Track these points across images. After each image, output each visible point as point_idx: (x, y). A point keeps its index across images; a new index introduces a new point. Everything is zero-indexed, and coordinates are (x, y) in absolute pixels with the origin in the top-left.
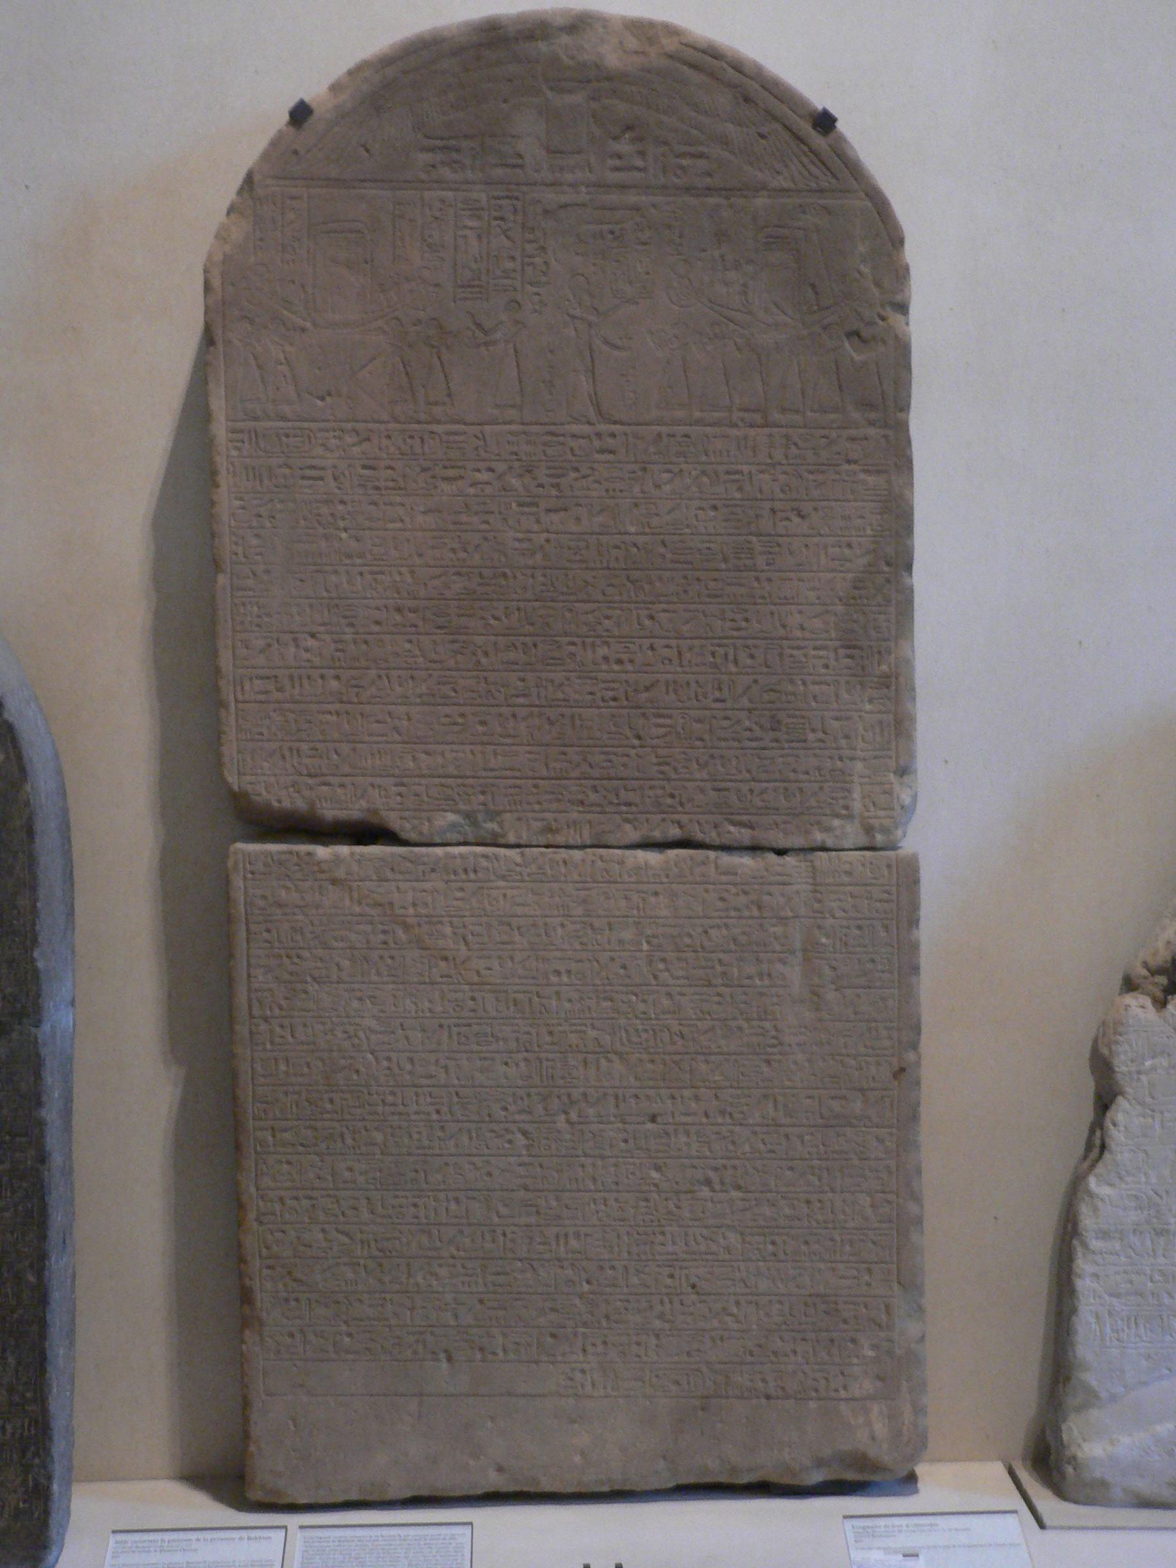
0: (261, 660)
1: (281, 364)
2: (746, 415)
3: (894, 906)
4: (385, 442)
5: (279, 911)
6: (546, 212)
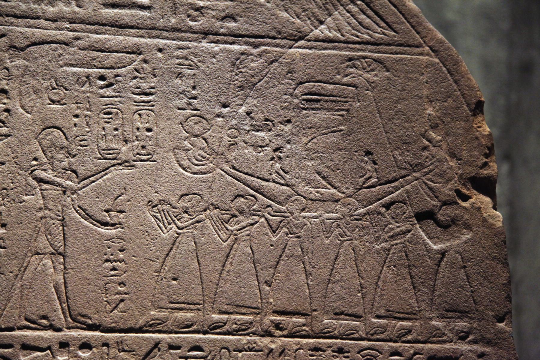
6: (12, 47)
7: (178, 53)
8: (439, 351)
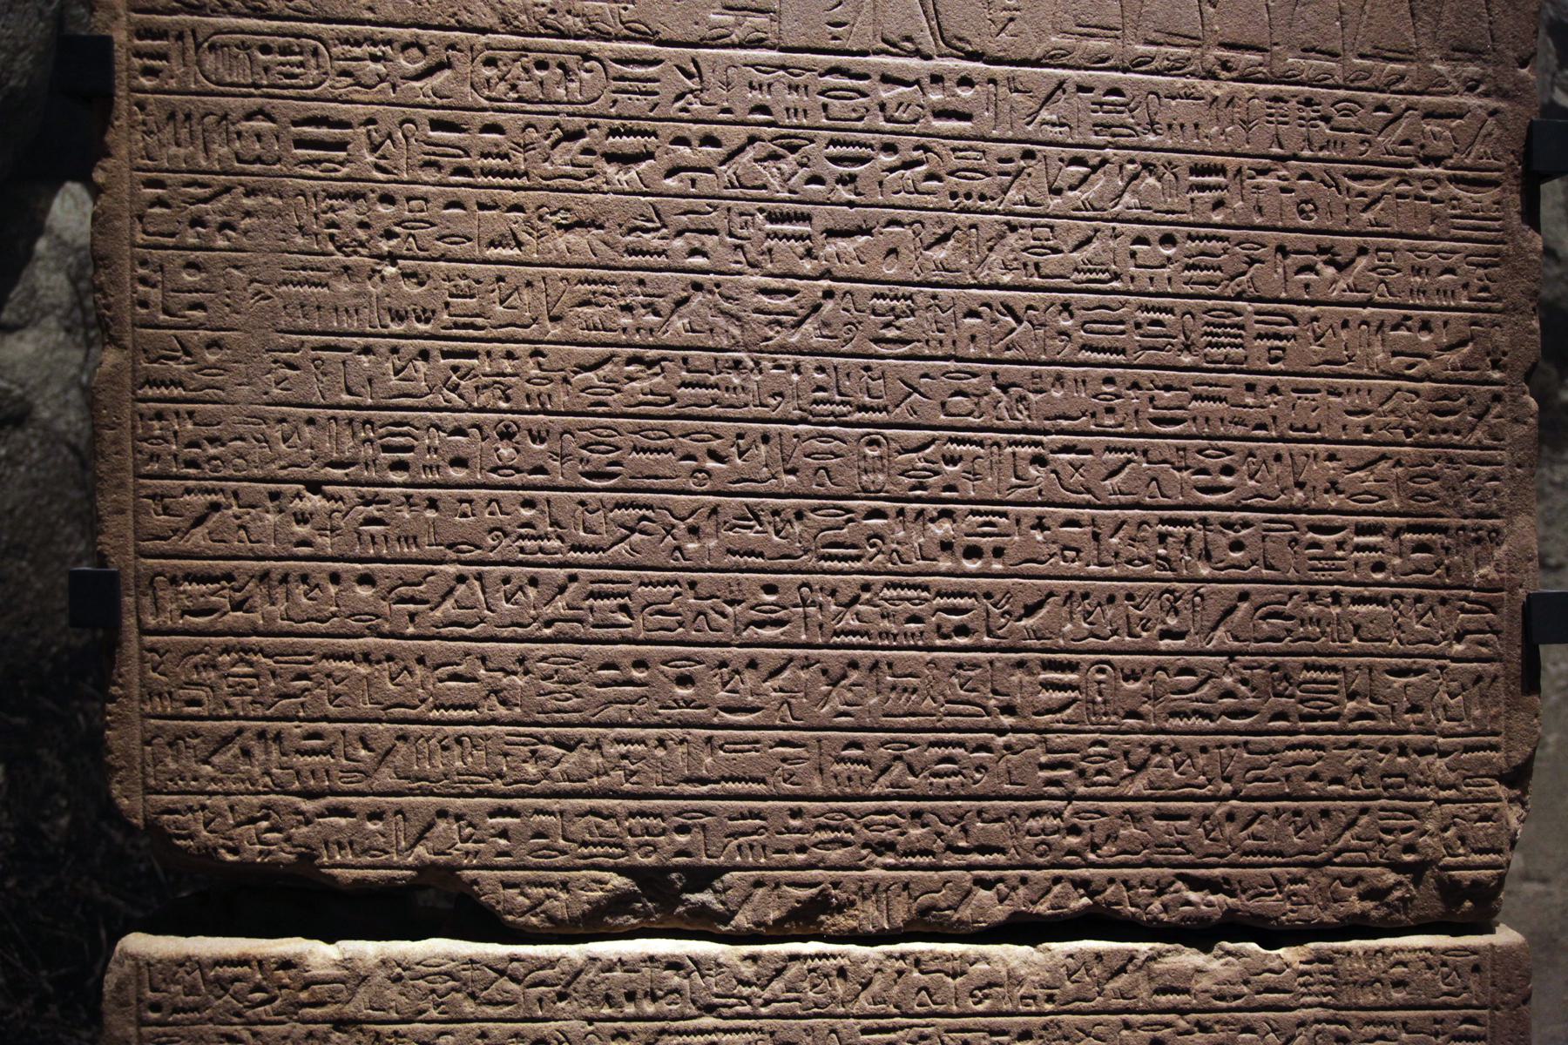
8: (1439, 106)
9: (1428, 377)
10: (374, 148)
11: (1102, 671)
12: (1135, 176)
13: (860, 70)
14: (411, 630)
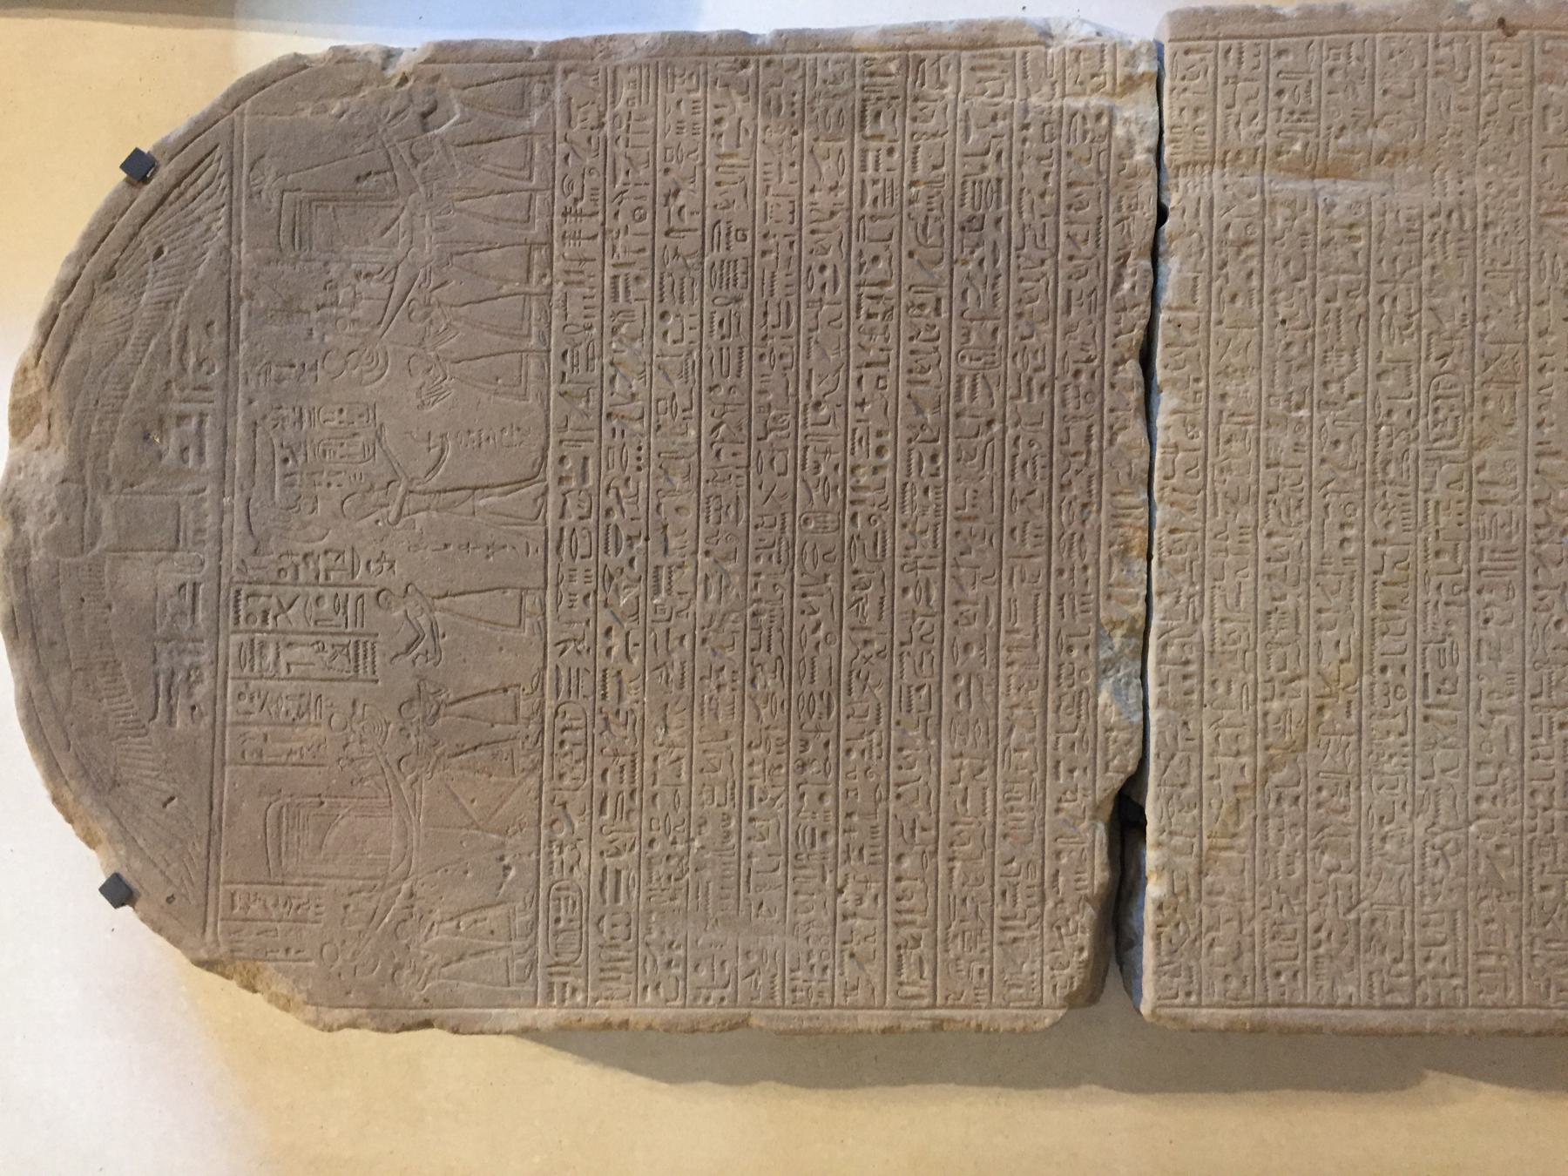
0: (873, 970)
1: (458, 926)
2: (535, 273)
3: (1246, 43)
4: (567, 782)
5: (1247, 956)
7: (252, 385)
9: (755, 118)
10: (618, 853)
11: (963, 357)
12: (620, 341)
13: (557, 534)
14: (933, 833)
